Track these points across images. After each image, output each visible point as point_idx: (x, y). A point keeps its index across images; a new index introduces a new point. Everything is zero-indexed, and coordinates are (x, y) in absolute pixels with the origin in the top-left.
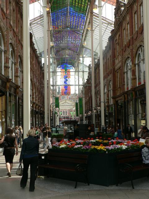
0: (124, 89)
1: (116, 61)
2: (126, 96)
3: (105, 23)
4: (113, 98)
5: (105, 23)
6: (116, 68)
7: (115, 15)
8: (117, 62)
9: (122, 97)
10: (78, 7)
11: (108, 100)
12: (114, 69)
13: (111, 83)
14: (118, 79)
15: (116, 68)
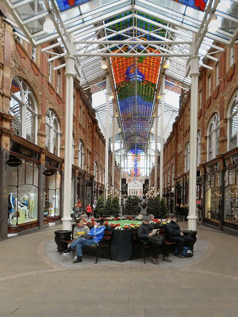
0: (183, 171)
1: (178, 145)
2: (185, 177)
3: (170, 110)
4: (175, 180)
5: (170, 110)
6: (179, 152)
7: (180, 102)
8: (179, 146)
9: (182, 179)
10: (145, 95)
11: (171, 181)
12: (176, 153)
13: (174, 167)
14: (179, 163)
15: (179, 152)
